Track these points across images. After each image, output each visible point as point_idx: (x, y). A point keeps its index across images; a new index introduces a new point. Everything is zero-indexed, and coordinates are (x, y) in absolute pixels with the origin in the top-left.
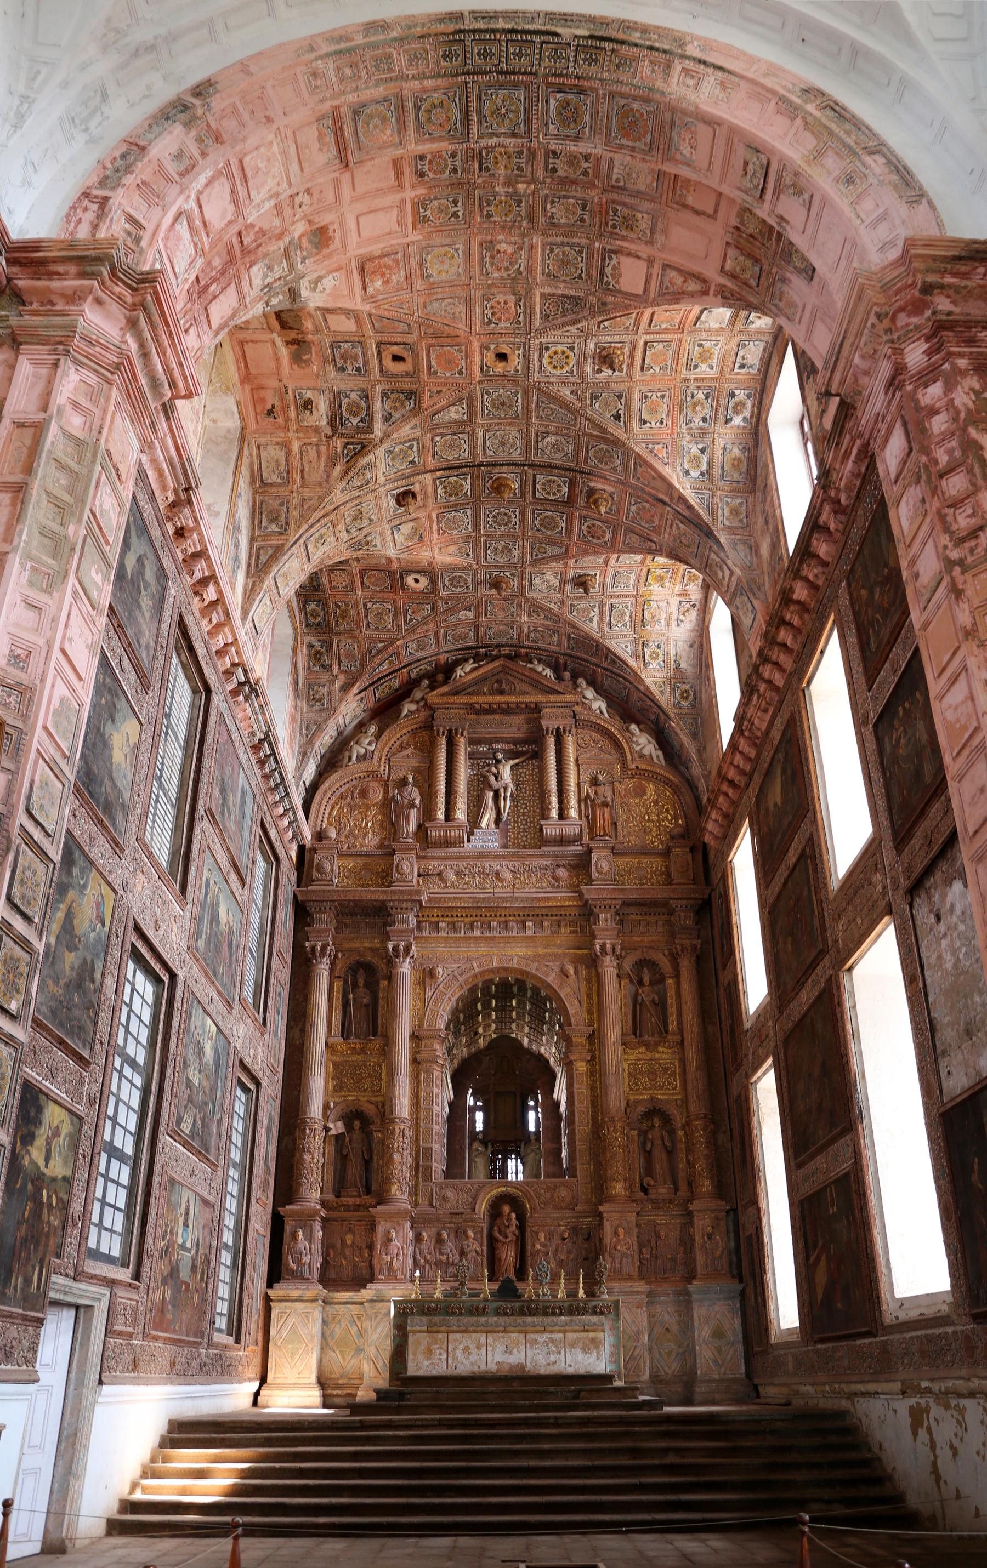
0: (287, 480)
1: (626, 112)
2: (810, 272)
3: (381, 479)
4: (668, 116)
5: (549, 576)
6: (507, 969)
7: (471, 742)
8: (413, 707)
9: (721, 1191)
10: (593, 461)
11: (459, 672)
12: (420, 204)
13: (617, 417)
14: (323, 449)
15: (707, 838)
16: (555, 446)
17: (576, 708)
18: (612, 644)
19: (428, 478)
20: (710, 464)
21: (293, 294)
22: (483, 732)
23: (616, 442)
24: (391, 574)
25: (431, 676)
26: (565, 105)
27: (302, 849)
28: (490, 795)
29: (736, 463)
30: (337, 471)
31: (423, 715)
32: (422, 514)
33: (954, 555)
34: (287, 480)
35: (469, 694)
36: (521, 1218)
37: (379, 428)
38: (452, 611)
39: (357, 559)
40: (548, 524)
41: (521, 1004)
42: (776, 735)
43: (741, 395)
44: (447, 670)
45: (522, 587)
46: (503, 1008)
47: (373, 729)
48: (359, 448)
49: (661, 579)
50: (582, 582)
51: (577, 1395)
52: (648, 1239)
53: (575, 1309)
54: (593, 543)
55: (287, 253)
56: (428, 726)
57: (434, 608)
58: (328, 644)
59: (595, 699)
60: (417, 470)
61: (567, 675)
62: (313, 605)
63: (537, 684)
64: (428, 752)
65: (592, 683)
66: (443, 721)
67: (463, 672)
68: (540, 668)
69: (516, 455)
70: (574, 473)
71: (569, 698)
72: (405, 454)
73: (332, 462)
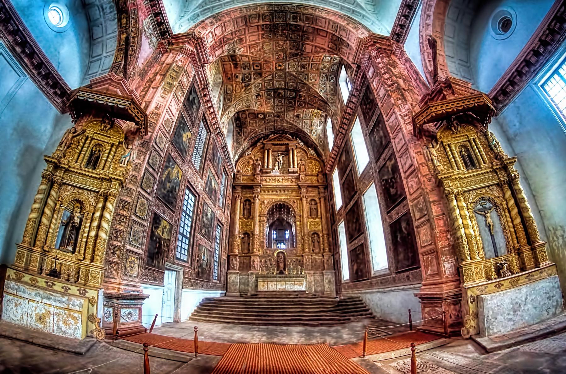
1: (306, 17)
2: (348, 46)
4: (315, 18)
5: (290, 115)
7: (273, 151)
10: (300, 88)
12: (262, 34)
13: (306, 79)
15: (327, 172)
16: (292, 85)
19: (263, 92)
21: (234, 51)
22: (276, 149)
24: (255, 114)
26: (293, 16)
27: (234, 174)
28: (277, 163)
30: (243, 90)
31: (262, 146)
32: (262, 100)
34: (232, 92)
36: (284, 256)
37: (253, 81)
38: (269, 122)
39: (247, 110)
40: (290, 102)
41: (284, 210)
42: (343, 145)
43: (333, 76)
46: (280, 211)
47: (251, 149)
49: (315, 116)
50: (298, 116)
51: (297, 295)
54: (300, 106)
55: (233, 43)
56: (263, 148)
58: (241, 130)
62: (238, 122)
71: (295, 142)
72: (258, 87)
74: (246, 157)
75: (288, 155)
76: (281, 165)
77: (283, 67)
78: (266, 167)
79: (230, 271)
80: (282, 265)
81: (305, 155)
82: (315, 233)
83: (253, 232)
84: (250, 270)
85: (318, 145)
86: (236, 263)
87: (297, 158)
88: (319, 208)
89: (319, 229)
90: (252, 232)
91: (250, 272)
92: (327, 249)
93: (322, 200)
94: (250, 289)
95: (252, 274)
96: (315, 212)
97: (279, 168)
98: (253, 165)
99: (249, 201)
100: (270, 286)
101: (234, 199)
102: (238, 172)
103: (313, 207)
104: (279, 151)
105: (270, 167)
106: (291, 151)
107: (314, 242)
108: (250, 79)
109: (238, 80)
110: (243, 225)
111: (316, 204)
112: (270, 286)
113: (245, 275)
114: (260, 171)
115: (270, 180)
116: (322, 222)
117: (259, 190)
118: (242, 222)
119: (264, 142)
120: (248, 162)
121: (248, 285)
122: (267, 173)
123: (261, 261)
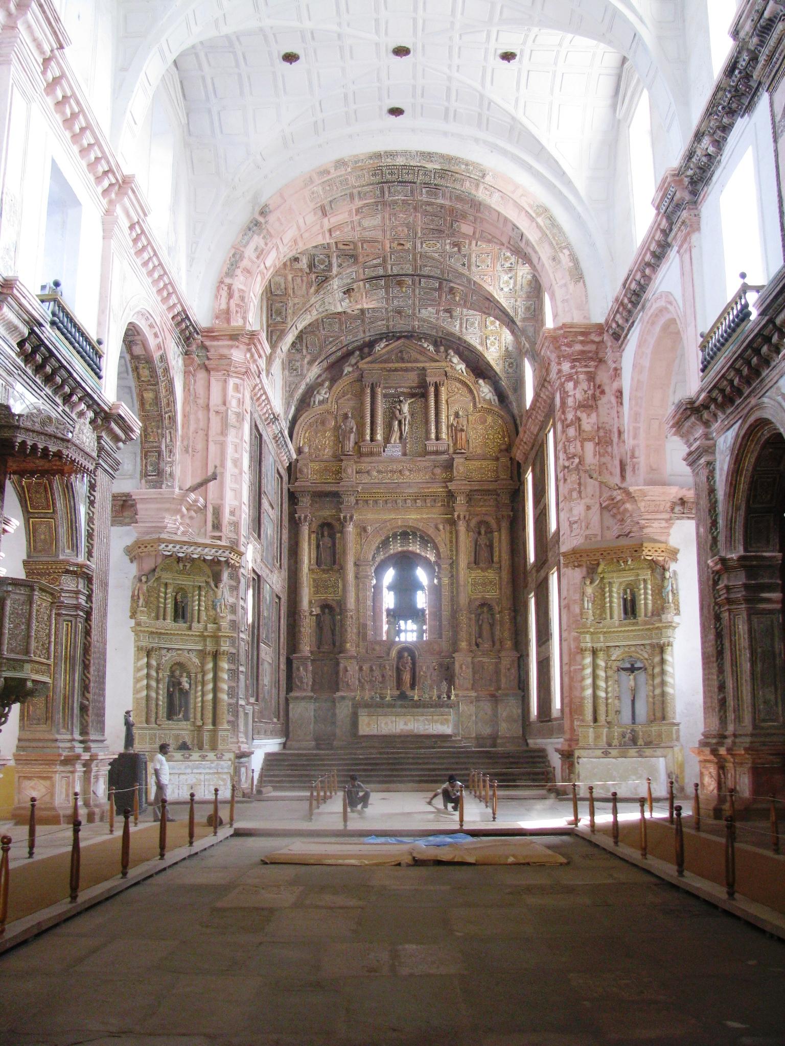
3: (335, 287)
6: (406, 526)
8: (350, 369)
11: (377, 348)
13: (464, 265)
14: (305, 279)
17: (447, 369)
19: (361, 283)
23: (463, 274)
25: (360, 349)
29: (530, 283)
30: (312, 290)
31: (356, 375)
33: (567, 464)
35: (385, 361)
37: (335, 270)
38: (373, 323)
44: (371, 344)
45: (414, 314)
48: (323, 280)
52: (477, 669)
53: (439, 705)
56: (360, 379)
57: (363, 321)
59: (459, 363)
61: (442, 349)
63: (423, 352)
64: (360, 396)
66: (368, 381)
67: (380, 347)
68: (425, 345)
69: (410, 272)
70: (441, 280)
73: (310, 285)
77: (408, 246)
78: (368, 438)
79: (292, 694)
80: (407, 677)
82: (484, 604)
83: (342, 603)
84: (338, 690)
86: (305, 674)
88: (496, 544)
89: (492, 594)
91: (339, 694)
92: (509, 644)
93: (505, 524)
94: (338, 731)
95: (343, 698)
96: (484, 554)
97: (401, 438)
98: (337, 428)
100: (383, 725)
101: (294, 524)
102: (299, 451)
103: (483, 540)
104: (400, 387)
105: (379, 437)
106: (432, 390)
107: (480, 627)
109: (297, 266)
110: (318, 586)
111: (492, 532)
112: (383, 725)
114: (353, 448)
115: (378, 472)
116: (500, 578)
117: (353, 500)
118: (314, 580)
119: (362, 365)
120: (323, 423)
121: (334, 723)
122: (371, 454)
123: (361, 669)
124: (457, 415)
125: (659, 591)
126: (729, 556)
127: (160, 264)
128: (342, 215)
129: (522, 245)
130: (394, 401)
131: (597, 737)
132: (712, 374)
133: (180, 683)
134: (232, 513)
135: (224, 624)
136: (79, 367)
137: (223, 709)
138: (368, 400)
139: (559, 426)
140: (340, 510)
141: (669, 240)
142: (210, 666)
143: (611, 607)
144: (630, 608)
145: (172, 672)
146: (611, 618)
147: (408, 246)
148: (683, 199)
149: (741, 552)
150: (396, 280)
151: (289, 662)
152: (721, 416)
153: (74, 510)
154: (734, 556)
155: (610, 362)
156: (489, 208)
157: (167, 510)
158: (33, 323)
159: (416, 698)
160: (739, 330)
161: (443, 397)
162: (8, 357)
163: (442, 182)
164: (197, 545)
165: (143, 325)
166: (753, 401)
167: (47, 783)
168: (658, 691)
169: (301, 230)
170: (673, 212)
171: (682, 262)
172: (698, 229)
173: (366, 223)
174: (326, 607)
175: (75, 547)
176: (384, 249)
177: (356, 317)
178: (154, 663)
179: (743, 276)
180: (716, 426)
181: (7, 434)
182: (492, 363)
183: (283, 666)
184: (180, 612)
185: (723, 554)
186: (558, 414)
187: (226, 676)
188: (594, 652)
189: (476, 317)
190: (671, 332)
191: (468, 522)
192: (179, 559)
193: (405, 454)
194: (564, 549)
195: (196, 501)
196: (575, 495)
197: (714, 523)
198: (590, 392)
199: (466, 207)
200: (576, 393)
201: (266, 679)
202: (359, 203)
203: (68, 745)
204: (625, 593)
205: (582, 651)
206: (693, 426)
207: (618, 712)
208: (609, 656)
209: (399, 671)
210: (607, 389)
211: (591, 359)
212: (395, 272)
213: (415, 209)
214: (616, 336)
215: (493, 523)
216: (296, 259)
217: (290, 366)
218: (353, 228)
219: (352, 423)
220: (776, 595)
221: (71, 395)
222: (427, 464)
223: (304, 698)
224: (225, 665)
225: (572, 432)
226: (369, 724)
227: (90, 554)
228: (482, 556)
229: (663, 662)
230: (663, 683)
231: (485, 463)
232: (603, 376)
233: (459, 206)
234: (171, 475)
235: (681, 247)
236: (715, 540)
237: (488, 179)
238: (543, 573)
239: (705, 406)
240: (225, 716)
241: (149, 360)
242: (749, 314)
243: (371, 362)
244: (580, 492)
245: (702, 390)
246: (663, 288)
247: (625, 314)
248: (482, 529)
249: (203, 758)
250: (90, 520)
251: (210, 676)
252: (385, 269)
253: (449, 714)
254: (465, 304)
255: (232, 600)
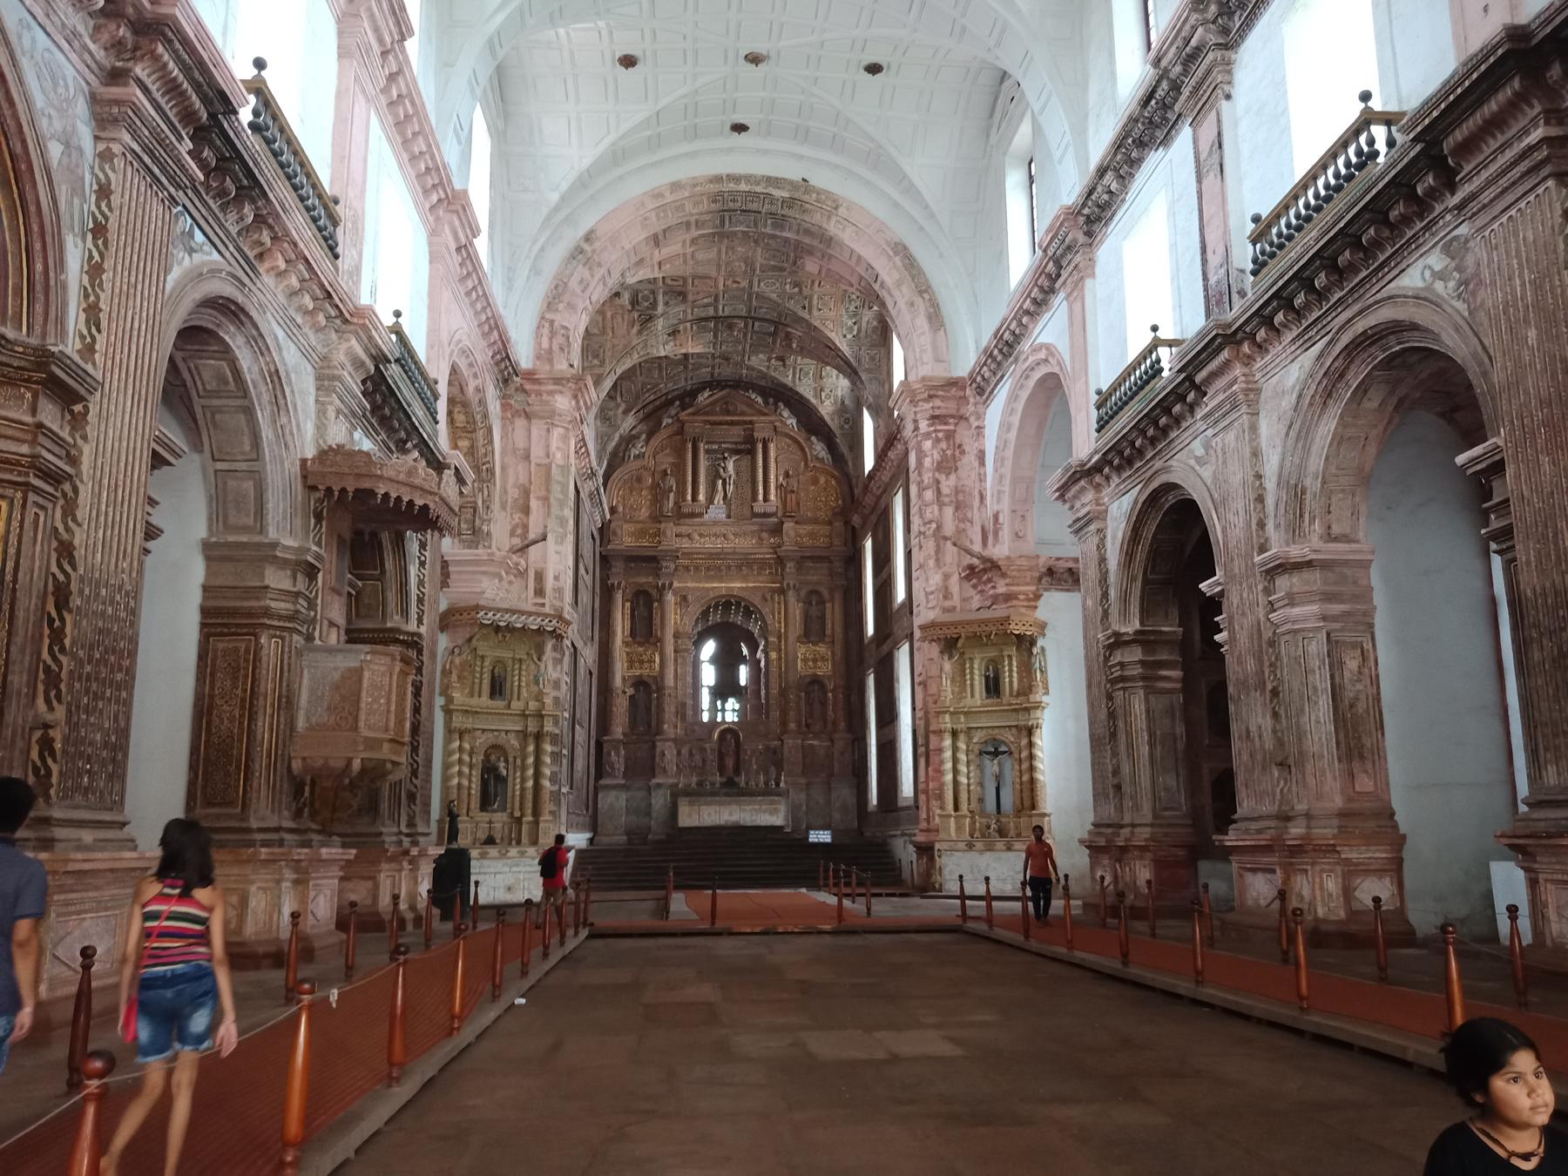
0: (603, 332)
9: (850, 728)
11: (700, 398)
18: (801, 390)
20: (859, 330)
25: (681, 397)
29: (875, 329)
35: (706, 414)
37: (660, 308)
44: (693, 394)
48: (647, 320)
52: (807, 752)
56: (681, 432)
60: (681, 322)
63: (751, 404)
64: (680, 453)
65: (788, 405)
67: (704, 397)
70: (776, 324)
74: (633, 465)
75: (751, 452)
76: (731, 489)
79: (602, 782)
81: (798, 456)
82: (816, 681)
85: (837, 432)
86: (617, 760)
87: (776, 462)
89: (825, 669)
90: (655, 678)
92: (842, 725)
93: (838, 596)
95: (659, 786)
98: (655, 486)
99: (646, 594)
101: (607, 593)
102: (613, 510)
103: (814, 611)
105: (701, 497)
106: (760, 446)
108: (654, 305)
109: (617, 301)
111: (822, 602)
113: (639, 789)
115: (701, 535)
120: (639, 480)
121: (648, 814)
122: (692, 515)
123: (679, 753)
124: (787, 475)
125: (1027, 670)
126: (1123, 630)
127: (485, 294)
128: (673, 248)
129: (876, 287)
130: (718, 458)
131: (959, 828)
132: (1110, 434)
133: (496, 769)
134: (556, 578)
135: (548, 701)
136: (418, 412)
137: (546, 796)
138: (690, 455)
139: (913, 489)
140: (658, 576)
141: (1057, 285)
142: (531, 748)
143: (972, 685)
144: (993, 686)
145: (487, 755)
146: (972, 696)
147: (744, 284)
148: (1075, 240)
149: (1137, 625)
150: (723, 322)
151: (599, 745)
152: (1115, 480)
153: (404, 571)
154: (1130, 630)
155: (972, 419)
156: (841, 245)
157: (484, 573)
158: (380, 359)
159: (743, 784)
160: (1147, 388)
161: (772, 454)
162: (354, 396)
163: (790, 213)
164: (522, 613)
165: (462, 364)
166: (1158, 464)
167: (369, 884)
168: (1026, 778)
169: (622, 264)
170: (1063, 256)
171: (1071, 310)
172: (1093, 275)
173: (700, 256)
174: (640, 684)
175: (405, 613)
176: (716, 286)
177: (677, 363)
178: (467, 746)
179: (1155, 329)
180: (1106, 491)
181: (366, 484)
182: (827, 418)
183: (593, 751)
184: (497, 688)
185: (1116, 627)
186: (913, 476)
187: (548, 760)
188: (954, 734)
189: (810, 365)
190: (1051, 389)
191: (797, 590)
192: (498, 629)
193: (729, 517)
194: (917, 622)
195: (517, 564)
196: (931, 563)
197: (1105, 595)
198: (949, 453)
199: (815, 243)
200: (931, 452)
201: (580, 764)
202: (695, 233)
203: (394, 838)
204: (987, 669)
205: (940, 732)
206: (1083, 489)
207: (981, 800)
208: (970, 738)
209: (721, 757)
210: (967, 448)
211: (952, 416)
212: (727, 313)
213: (756, 242)
214: (980, 391)
215: (826, 593)
216: (617, 294)
217: (604, 415)
218: (685, 262)
219: (672, 482)
220: (1176, 674)
221: (405, 442)
222: (755, 528)
223: (615, 787)
224: (548, 748)
225: (929, 495)
226: (690, 816)
227: (420, 621)
228: (813, 630)
229: (1031, 745)
230: (1032, 769)
231: (817, 527)
232: (964, 435)
233: (807, 240)
234: (489, 534)
235: (1069, 295)
236: (1106, 614)
237: (842, 211)
238: (885, 648)
239: (1097, 468)
240: (547, 806)
241: (465, 405)
242: (1161, 370)
243: (693, 414)
244: (937, 560)
245: (1096, 452)
246: (1044, 338)
247: (993, 366)
248: (813, 599)
249: (522, 854)
250: (421, 583)
251: (531, 760)
252: (716, 309)
253: (778, 803)
254: (802, 351)
255: (555, 676)
